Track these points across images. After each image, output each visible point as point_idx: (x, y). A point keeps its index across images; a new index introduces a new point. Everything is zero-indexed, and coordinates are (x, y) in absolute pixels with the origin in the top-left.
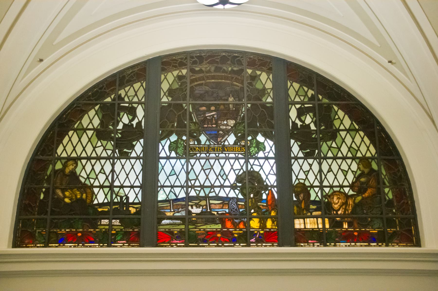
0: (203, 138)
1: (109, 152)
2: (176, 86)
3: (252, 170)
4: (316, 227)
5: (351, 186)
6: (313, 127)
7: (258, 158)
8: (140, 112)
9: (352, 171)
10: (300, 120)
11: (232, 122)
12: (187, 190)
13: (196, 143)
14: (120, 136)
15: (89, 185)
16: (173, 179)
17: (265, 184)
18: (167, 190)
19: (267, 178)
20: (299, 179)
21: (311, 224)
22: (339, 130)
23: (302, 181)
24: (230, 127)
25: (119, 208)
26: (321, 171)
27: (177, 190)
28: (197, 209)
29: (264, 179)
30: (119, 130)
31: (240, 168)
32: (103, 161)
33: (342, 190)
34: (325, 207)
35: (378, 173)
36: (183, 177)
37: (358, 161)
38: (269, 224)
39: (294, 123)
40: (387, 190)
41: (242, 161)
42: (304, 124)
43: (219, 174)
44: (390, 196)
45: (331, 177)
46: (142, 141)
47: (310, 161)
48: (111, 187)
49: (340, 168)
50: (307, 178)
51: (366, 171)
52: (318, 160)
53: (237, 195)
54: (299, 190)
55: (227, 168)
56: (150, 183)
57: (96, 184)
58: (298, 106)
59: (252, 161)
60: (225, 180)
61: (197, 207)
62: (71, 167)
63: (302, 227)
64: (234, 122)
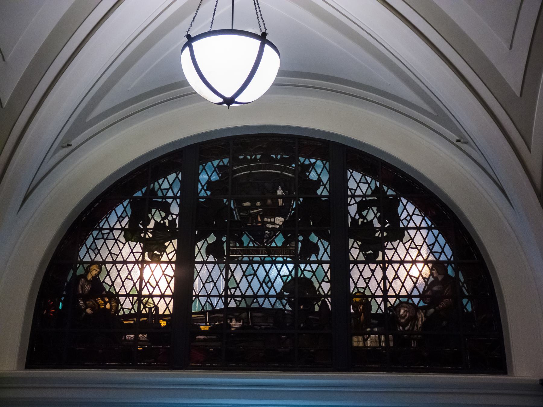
0: (245, 239)
1: (137, 255)
2: (215, 177)
3: (302, 276)
4: (378, 345)
5: (420, 296)
6: (376, 224)
7: (310, 263)
8: (175, 209)
10: (361, 216)
11: (279, 221)
12: (226, 300)
13: (238, 245)
14: (151, 235)
15: (115, 293)
17: (318, 293)
18: (203, 300)
19: (320, 286)
20: (358, 288)
22: (407, 228)
23: (362, 290)
24: (278, 227)
25: (148, 321)
26: (385, 278)
27: (214, 301)
28: (237, 323)
29: (317, 287)
30: (150, 229)
31: (288, 273)
32: (130, 266)
33: (410, 301)
34: (388, 320)
36: (221, 284)
40: (465, 301)
41: (291, 266)
42: (365, 221)
43: (264, 281)
44: (469, 308)
45: (397, 285)
46: (175, 242)
47: (373, 266)
48: (139, 295)
49: (408, 274)
50: (367, 286)
51: (440, 278)
52: (381, 265)
53: (284, 306)
54: (358, 300)
55: (273, 273)
56: (183, 292)
57: (122, 292)
58: (358, 199)
59: (302, 266)
60: (270, 289)
61: (237, 321)
62: (94, 272)
63: (361, 344)
64: (283, 220)
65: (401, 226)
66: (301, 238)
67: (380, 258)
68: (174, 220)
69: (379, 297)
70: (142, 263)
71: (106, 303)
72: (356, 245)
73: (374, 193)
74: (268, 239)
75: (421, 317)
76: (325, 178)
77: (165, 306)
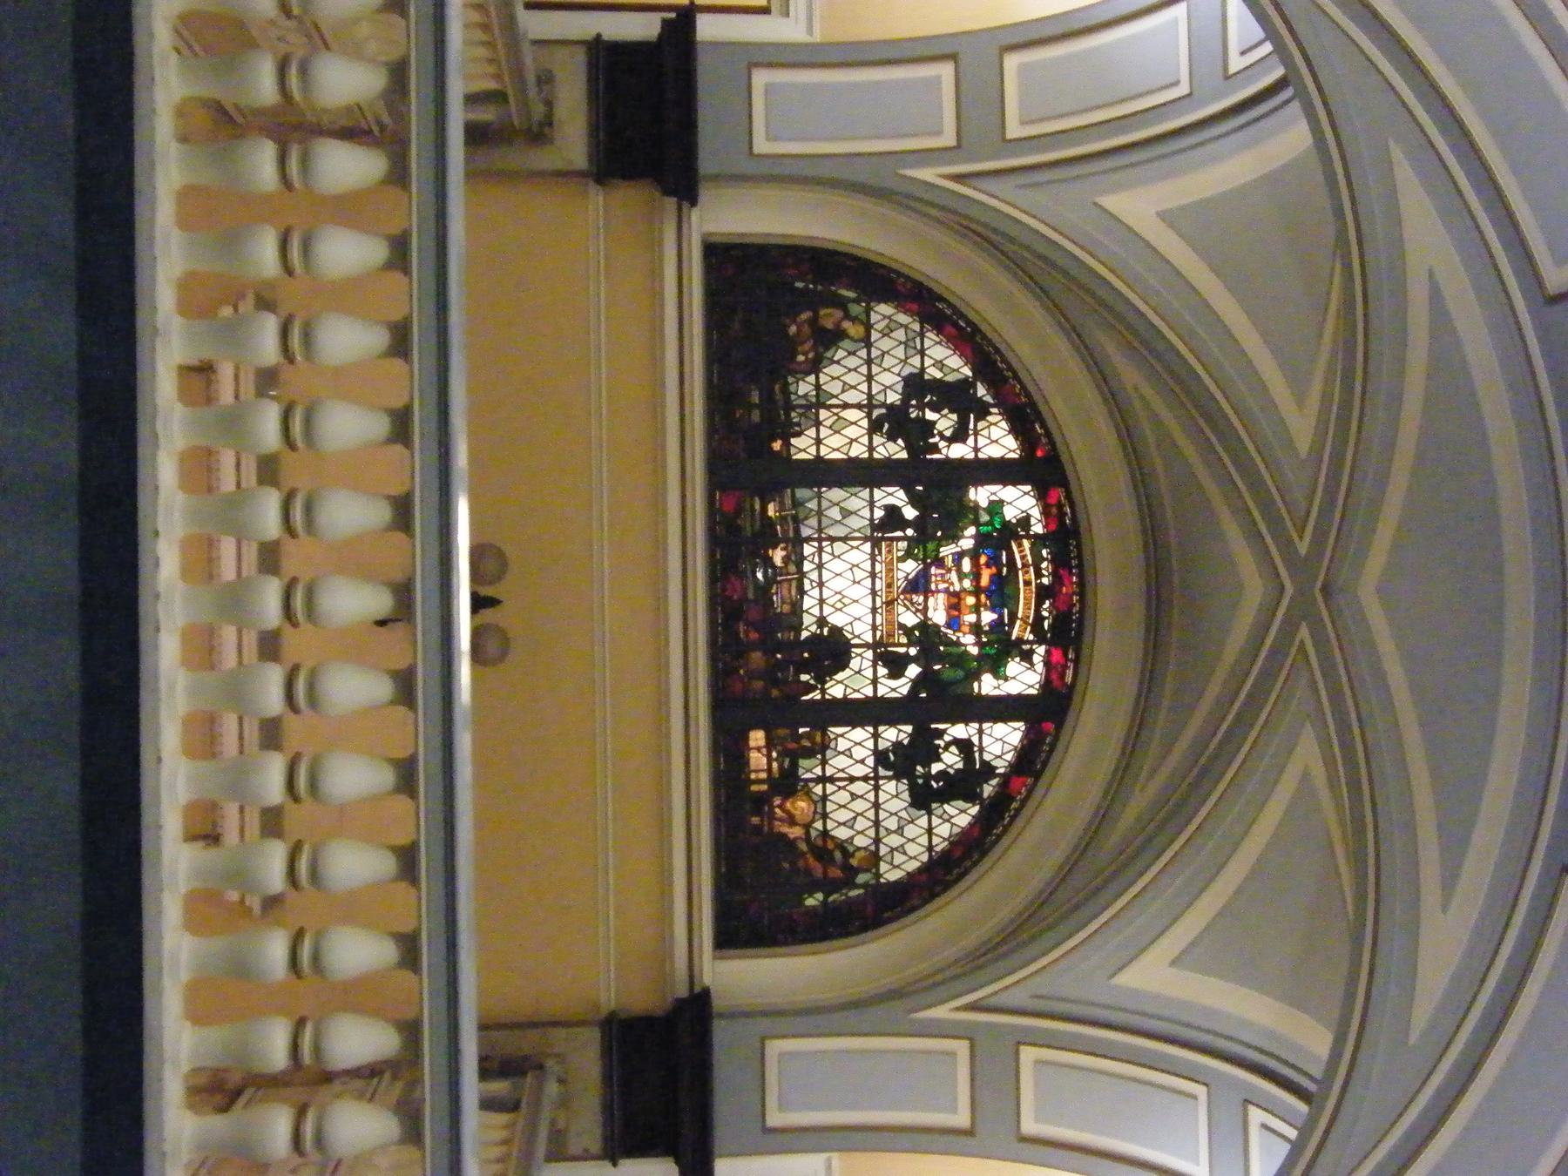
0: (911, 567)
1: (881, 398)
5: (825, 833)
6: (936, 768)
7: (875, 666)
9: (852, 838)
10: (948, 745)
11: (939, 616)
16: (835, 513)
21: (757, 760)
22: (930, 813)
23: (832, 745)
26: (852, 779)
27: (813, 522)
32: (864, 387)
34: (787, 783)
35: (849, 883)
37: (873, 848)
38: (758, 685)
39: (944, 731)
41: (869, 638)
44: (810, 902)
45: (843, 797)
46: (904, 455)
47: (870, 761)
48: (820, 404)
51: (854, 862)
54: (818, 739)
55: (855, 610)
58: (975, 740)
59: (869, 654)
63: (752, 744)
65: (934, 805)
66: (913, 651)
67: (882, 772)
68: (939, 451)
69: (823, 770)
70: (868, 406)
71: (805, 354)
72: (902, 736)
73: (985, 764)
74: (911, 601)
75: (795, 832)
76: (1012, 688)
77: (803, 447)
